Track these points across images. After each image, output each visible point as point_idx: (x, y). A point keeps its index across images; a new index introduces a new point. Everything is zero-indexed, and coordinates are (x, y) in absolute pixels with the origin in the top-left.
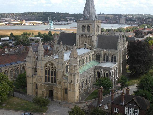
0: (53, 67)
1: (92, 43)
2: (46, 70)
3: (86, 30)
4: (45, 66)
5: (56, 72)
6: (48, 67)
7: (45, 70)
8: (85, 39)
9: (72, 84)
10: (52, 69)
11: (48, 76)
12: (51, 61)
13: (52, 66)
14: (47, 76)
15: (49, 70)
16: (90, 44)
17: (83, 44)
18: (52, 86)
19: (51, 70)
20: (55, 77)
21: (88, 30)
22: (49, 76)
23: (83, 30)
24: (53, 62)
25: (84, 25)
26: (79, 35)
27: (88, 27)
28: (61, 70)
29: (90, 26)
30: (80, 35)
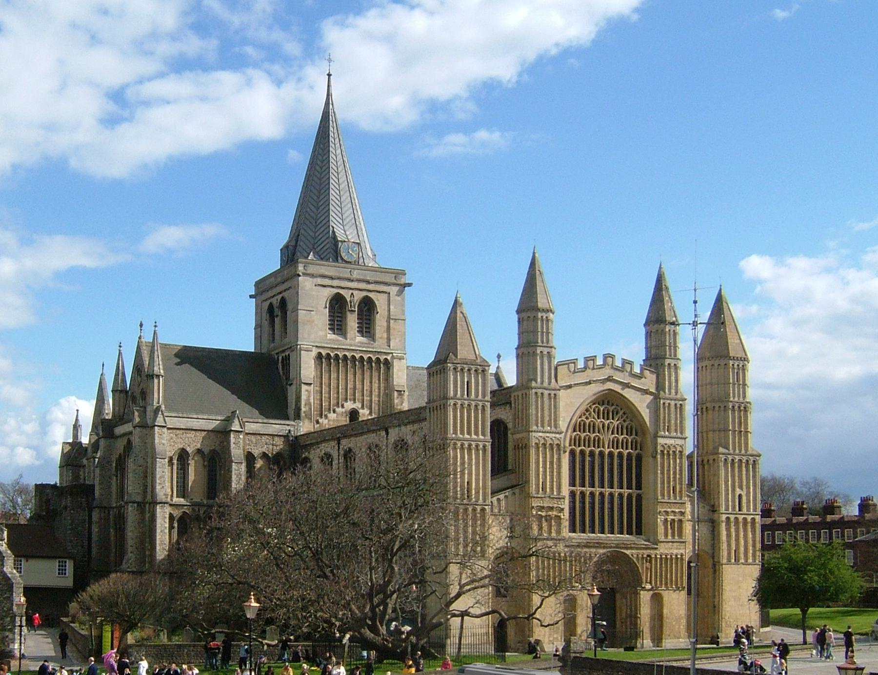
0: (619, 430)
1: (396, 401)
2: (578, 450)
3: (352, 321)
4: (579, 427)
5: (639, 458)
6: (593, 428)
7: (572, 452)
8: (350, 379)
9: (741, 517)
10: (615, 444)
11: (588, 490)
12: (617, 388)
13: (616, 423)
14: (583, 494)
15: (597, 451)
17: (339, 410)
18: (628, 552)
19: (607, 451)
20: (634, 492)
21: (367, 327)
22: (597, 490)
23: (337, 324)
24: (628, 394)
25: (342, 292)
26: (315, 352)
27: (367, 308)
28: (679, 442)
29: (380, 301)
30: (320, 354)
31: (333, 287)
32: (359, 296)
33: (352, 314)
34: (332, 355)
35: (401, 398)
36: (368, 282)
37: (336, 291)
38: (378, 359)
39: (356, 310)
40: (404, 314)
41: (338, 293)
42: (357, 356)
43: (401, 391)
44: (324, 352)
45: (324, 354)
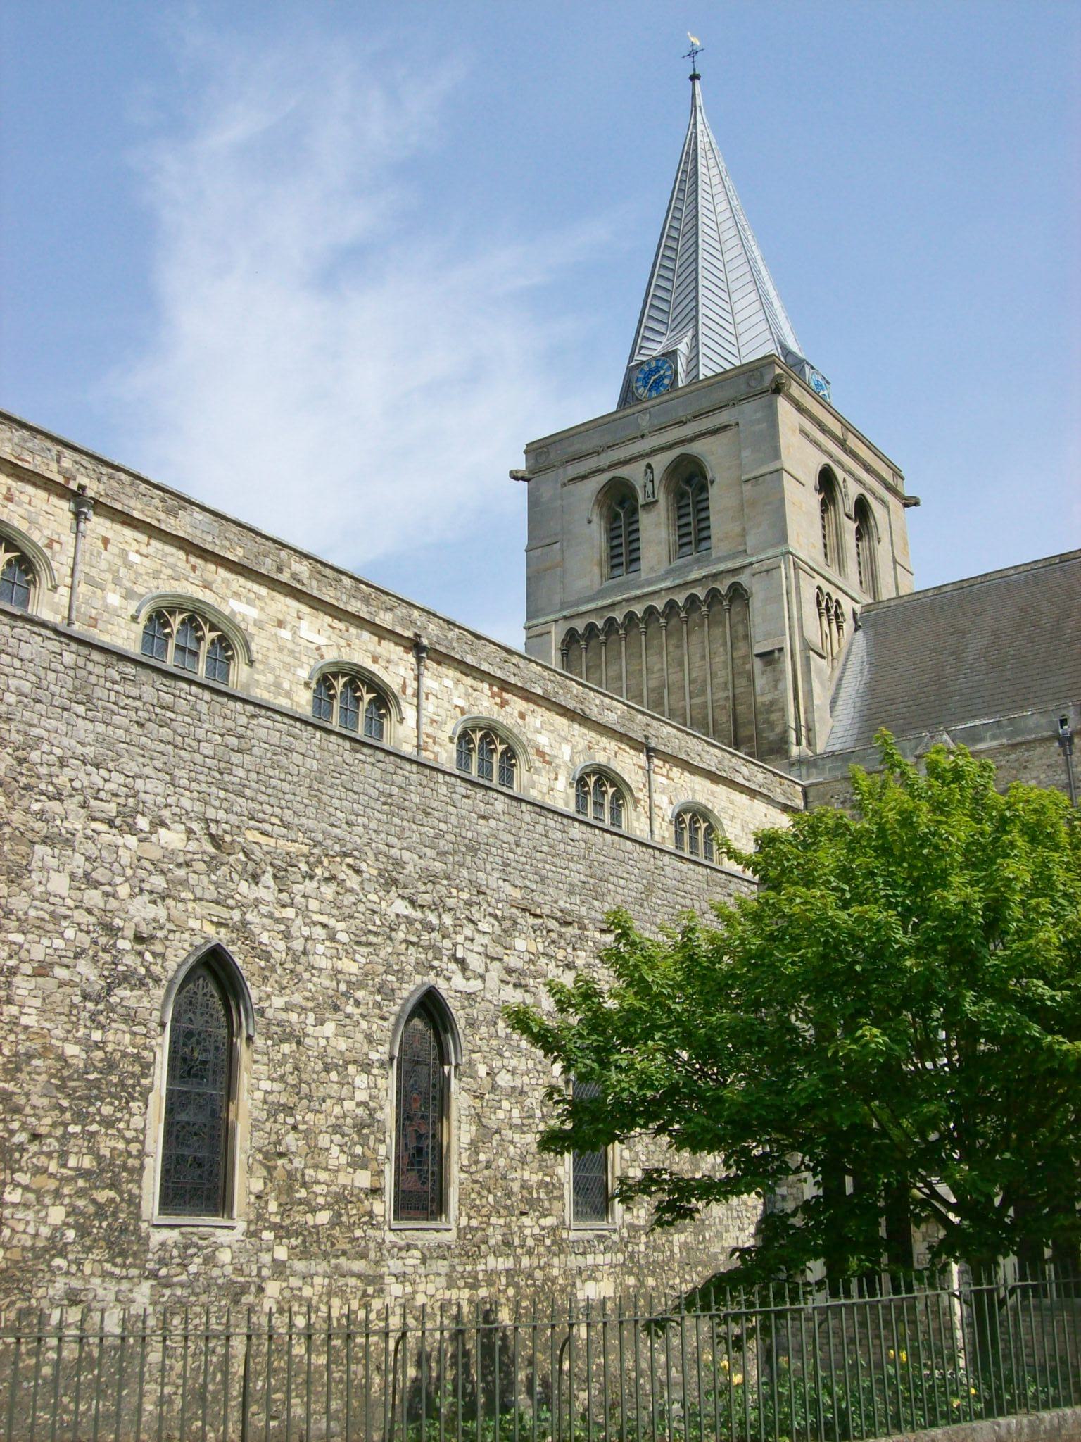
1: (760, 682)
16: (724, 718)
25: (622, 472)
29: (711, 452)
30: (571, 633)
31: (599, 471)
32: (661, 462)
33: (649, 511)
34: (600, 624)
35: (774, 670)
36: (683, 423)
37: (605, 478)
38: (713, 593)
39: (661, 496)
40: (777, 456)
41: (614, 478)
42: (659, 605)
43: (772, 652)
44: (580, 625)
45: (581, 630)
